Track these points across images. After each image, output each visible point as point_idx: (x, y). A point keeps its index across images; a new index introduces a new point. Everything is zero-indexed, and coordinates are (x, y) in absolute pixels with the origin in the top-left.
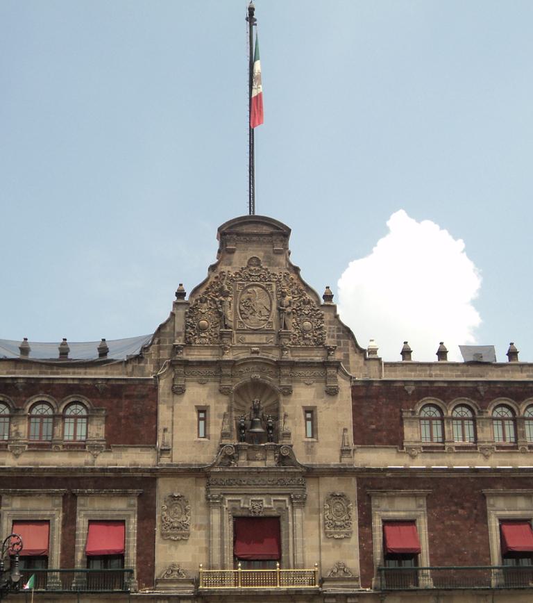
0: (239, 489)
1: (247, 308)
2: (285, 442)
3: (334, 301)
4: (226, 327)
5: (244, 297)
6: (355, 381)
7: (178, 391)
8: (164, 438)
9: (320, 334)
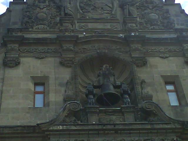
4: (66, 14)
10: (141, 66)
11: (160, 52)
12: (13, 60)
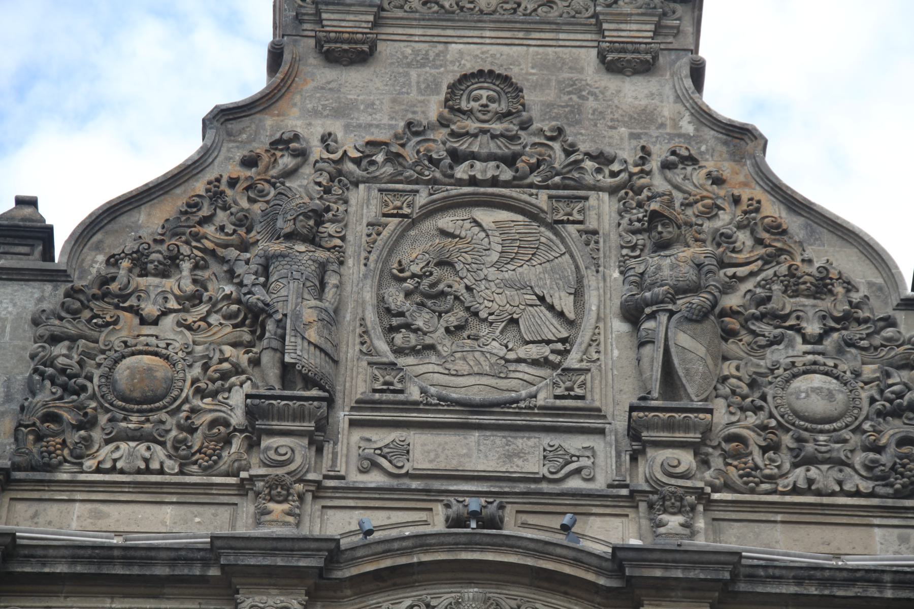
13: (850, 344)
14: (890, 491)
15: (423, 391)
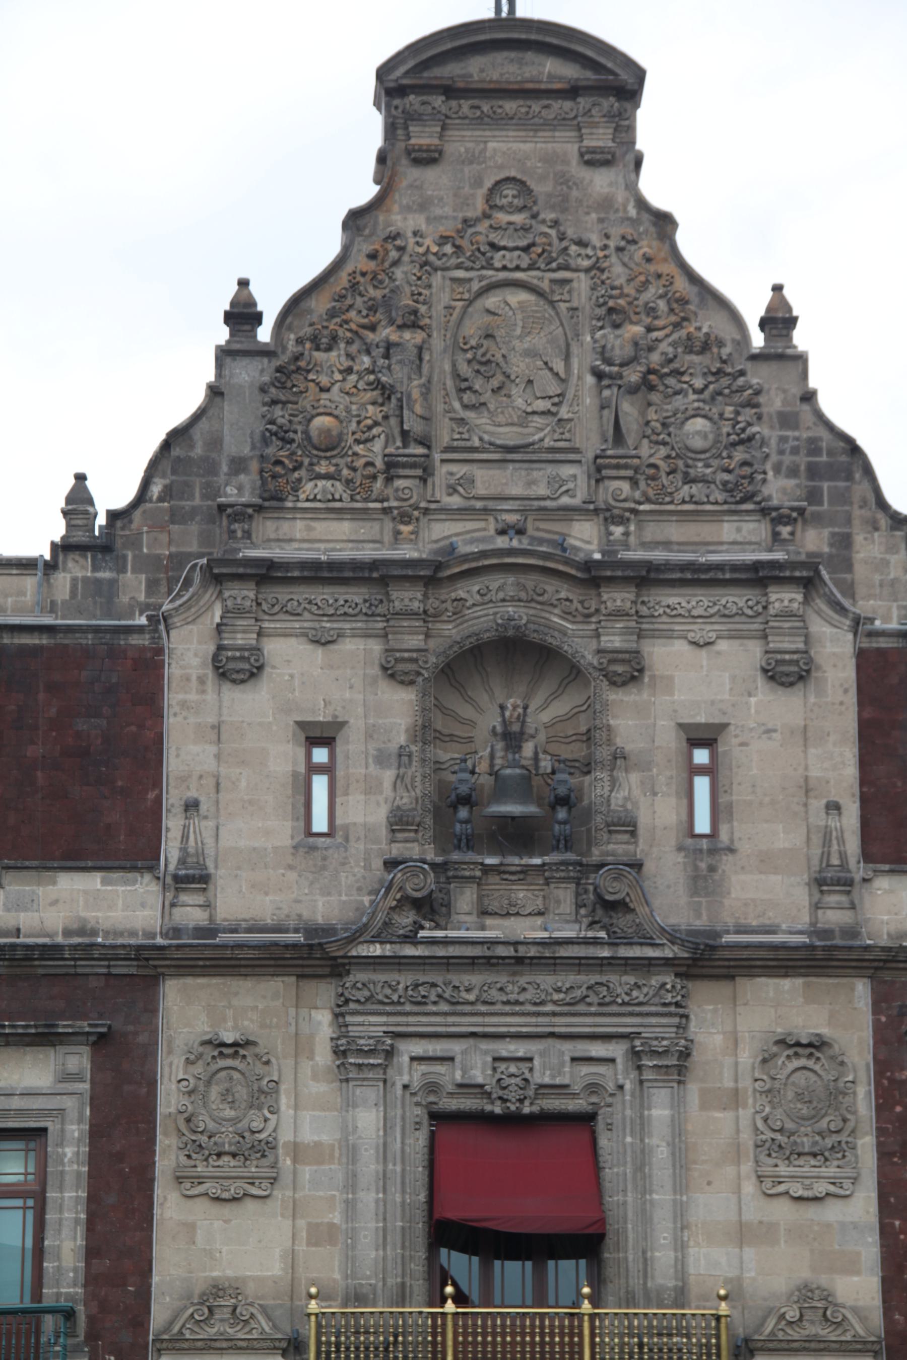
0: (451, 1019)
1: (483, 369)
2: (616, 847)
3: (802, 338)
5: (471, 329)
6: (871, 634)
7: (237, 668)
8: (185, 837)
9: (745, 463)
10: (624, 684)
11: (693, 617)
12: (242, 658)
13: (720, 393)
14: (733, 500)
15: (481, 439)
